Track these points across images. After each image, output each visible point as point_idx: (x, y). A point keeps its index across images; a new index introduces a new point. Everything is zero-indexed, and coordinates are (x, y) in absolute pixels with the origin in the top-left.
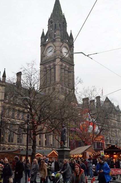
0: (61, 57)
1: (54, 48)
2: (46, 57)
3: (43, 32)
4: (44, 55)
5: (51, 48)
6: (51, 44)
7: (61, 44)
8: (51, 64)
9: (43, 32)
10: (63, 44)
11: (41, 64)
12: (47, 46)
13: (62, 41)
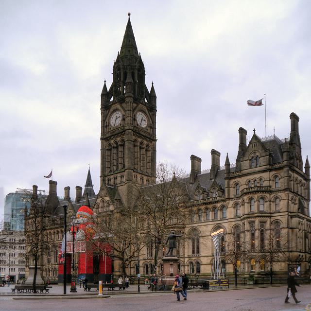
0: (134, 127)
1: (124, 113)
2: (110, 127)
3: (105, 86)
4: (107, 124)
5: (117, 112)
6: (118, 106)
7: (135, 105)
8: (119, 139)
9: (105, 86)
10: (136, 107)
11: (101, 139)
12: (111, 110)
13: (137, 100)
